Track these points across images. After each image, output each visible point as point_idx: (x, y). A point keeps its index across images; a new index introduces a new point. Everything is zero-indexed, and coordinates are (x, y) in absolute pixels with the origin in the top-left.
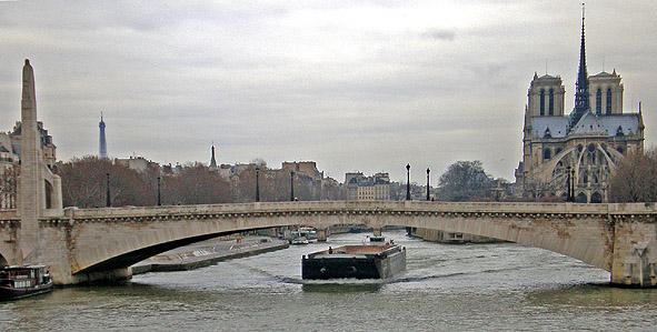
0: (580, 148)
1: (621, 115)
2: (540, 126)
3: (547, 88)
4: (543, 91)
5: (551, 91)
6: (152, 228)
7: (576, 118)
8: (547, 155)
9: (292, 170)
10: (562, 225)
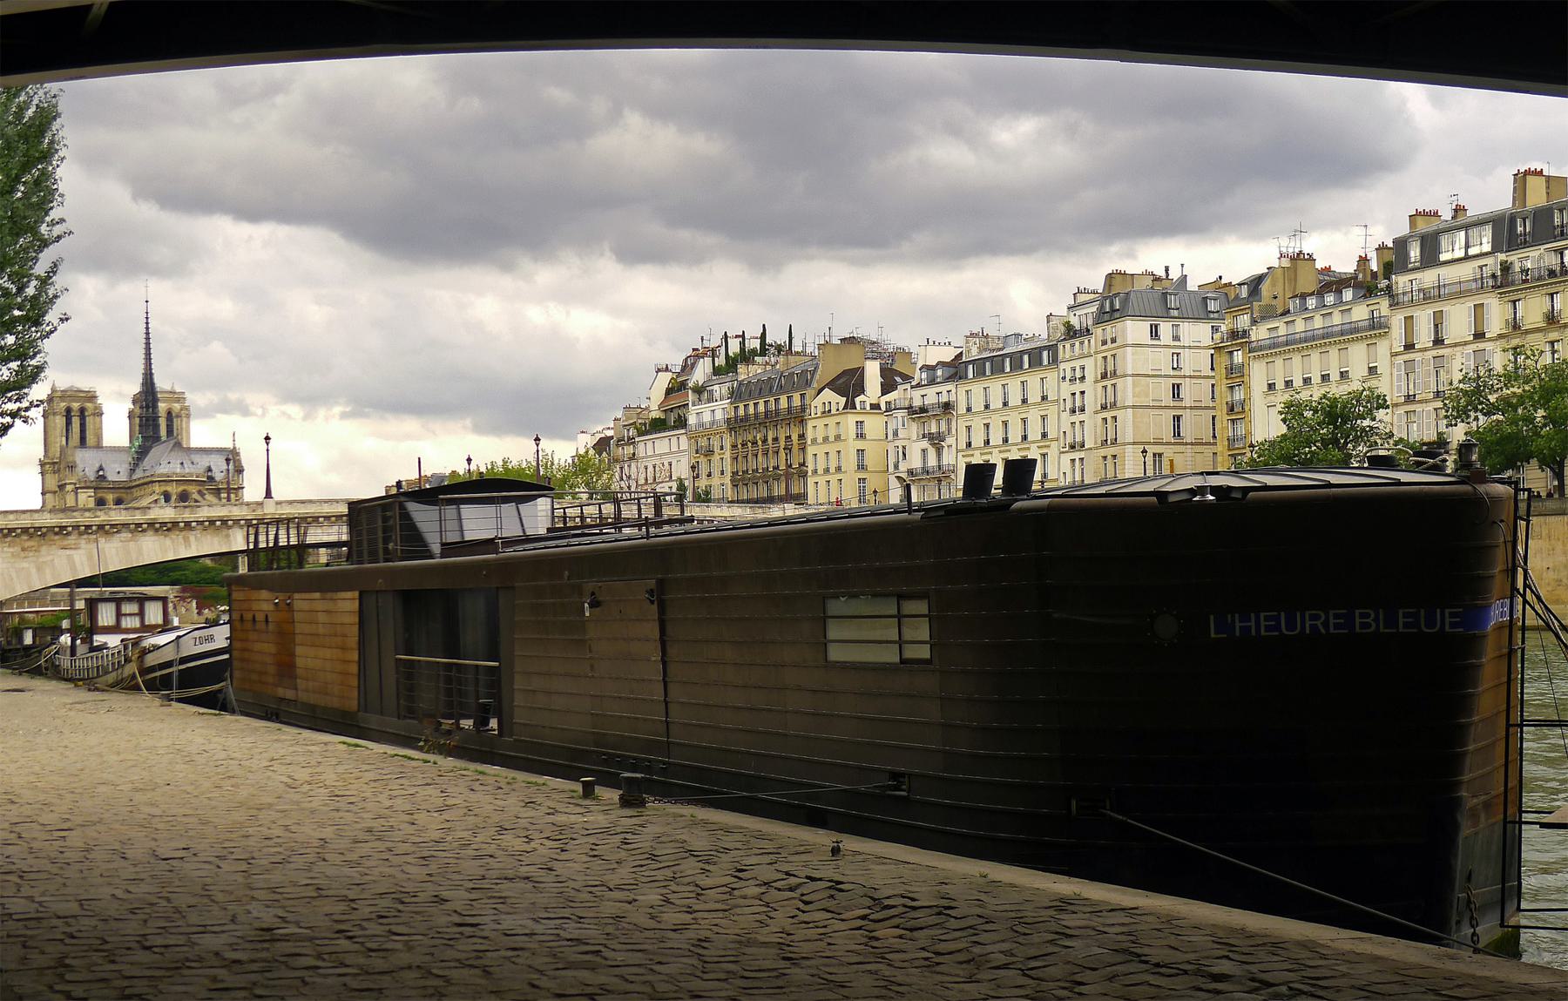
1: (189, 449)
2: (86, 462)
3: (76, 406)
4: (68, 410)
5: (82, 411)
7: (142, 453)
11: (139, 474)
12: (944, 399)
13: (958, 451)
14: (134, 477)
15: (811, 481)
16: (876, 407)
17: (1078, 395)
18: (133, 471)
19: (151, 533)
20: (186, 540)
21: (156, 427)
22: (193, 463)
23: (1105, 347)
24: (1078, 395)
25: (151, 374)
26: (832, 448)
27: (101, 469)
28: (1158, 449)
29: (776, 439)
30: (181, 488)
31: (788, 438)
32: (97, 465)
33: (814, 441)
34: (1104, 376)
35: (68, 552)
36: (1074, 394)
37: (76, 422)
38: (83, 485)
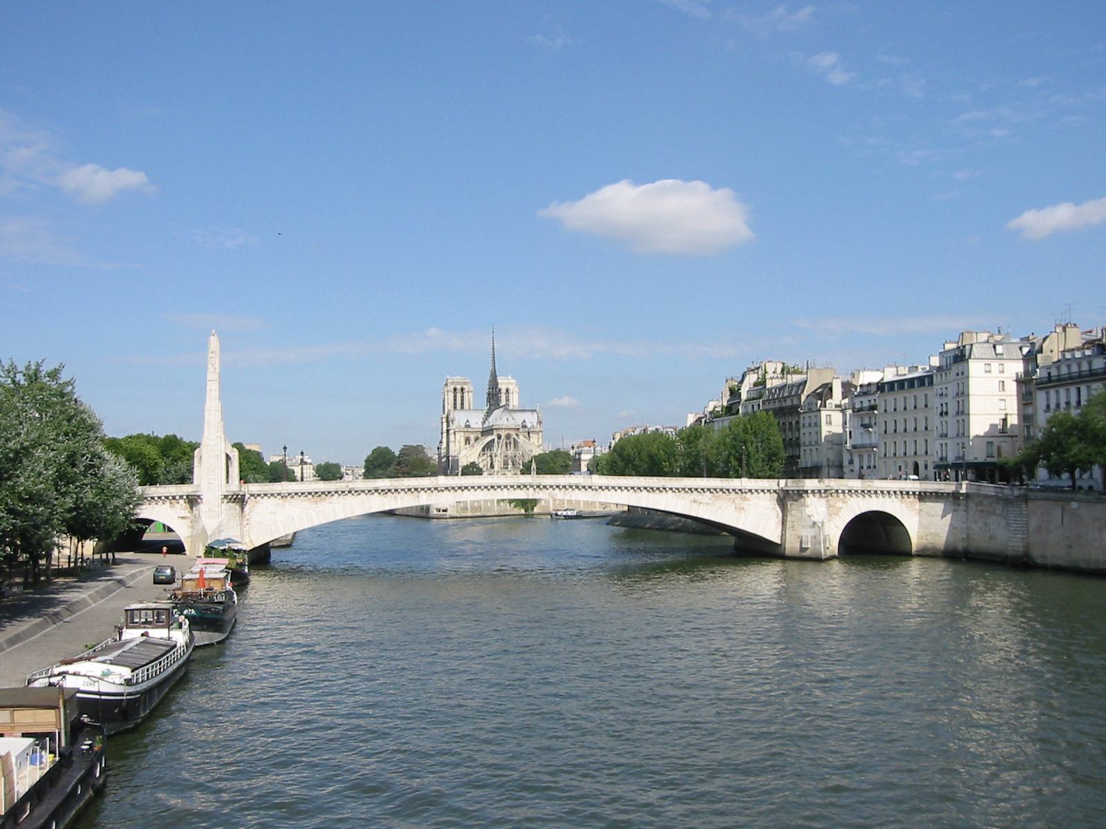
0: (499, 437)
3: (459, 387)
4: (455, 389)
5: (462, 389)
6: (330, 503)
7: (489, 414)
8: (467, 440)
9: (406, 451)
10: (738, 501)
11: (486, 425)
12: (873, 403)
13: (879, 435)
14: (485, 426)
15: (802, 449)
16: (836, 406)
17: (944, 405)
18: (484, 423)
19: (376, 494)
20: (395, 498)
21: (498, 400)
22: (513, 419)
23: (958, 377)
24: (944, 405)
25: (495, 371)
26: (813, 430)
27: (468, 421)
28: (991, 440)
29: (783, 424)
30: (508, 432)
31: (791, 423)
32: (466, 420)
33: (804, 425)
34: (958, 394)
35: (333, 505)
36: (942, 405)
37: (459, 396)
38: (458, 430)
